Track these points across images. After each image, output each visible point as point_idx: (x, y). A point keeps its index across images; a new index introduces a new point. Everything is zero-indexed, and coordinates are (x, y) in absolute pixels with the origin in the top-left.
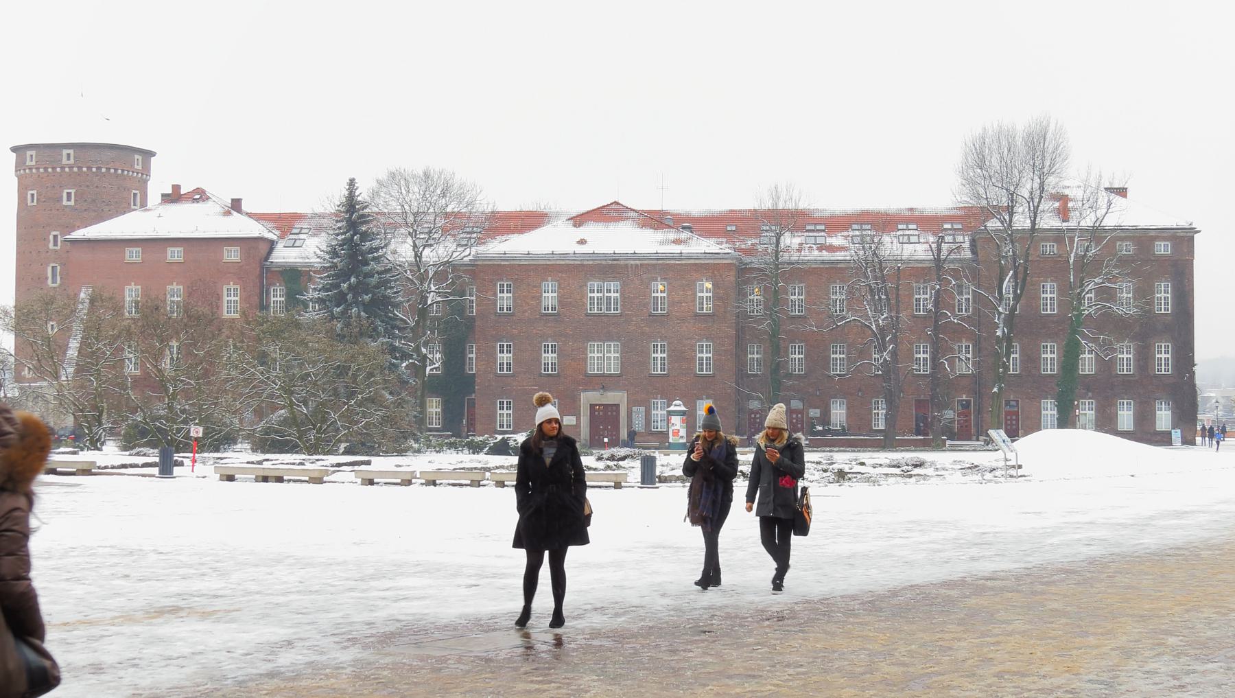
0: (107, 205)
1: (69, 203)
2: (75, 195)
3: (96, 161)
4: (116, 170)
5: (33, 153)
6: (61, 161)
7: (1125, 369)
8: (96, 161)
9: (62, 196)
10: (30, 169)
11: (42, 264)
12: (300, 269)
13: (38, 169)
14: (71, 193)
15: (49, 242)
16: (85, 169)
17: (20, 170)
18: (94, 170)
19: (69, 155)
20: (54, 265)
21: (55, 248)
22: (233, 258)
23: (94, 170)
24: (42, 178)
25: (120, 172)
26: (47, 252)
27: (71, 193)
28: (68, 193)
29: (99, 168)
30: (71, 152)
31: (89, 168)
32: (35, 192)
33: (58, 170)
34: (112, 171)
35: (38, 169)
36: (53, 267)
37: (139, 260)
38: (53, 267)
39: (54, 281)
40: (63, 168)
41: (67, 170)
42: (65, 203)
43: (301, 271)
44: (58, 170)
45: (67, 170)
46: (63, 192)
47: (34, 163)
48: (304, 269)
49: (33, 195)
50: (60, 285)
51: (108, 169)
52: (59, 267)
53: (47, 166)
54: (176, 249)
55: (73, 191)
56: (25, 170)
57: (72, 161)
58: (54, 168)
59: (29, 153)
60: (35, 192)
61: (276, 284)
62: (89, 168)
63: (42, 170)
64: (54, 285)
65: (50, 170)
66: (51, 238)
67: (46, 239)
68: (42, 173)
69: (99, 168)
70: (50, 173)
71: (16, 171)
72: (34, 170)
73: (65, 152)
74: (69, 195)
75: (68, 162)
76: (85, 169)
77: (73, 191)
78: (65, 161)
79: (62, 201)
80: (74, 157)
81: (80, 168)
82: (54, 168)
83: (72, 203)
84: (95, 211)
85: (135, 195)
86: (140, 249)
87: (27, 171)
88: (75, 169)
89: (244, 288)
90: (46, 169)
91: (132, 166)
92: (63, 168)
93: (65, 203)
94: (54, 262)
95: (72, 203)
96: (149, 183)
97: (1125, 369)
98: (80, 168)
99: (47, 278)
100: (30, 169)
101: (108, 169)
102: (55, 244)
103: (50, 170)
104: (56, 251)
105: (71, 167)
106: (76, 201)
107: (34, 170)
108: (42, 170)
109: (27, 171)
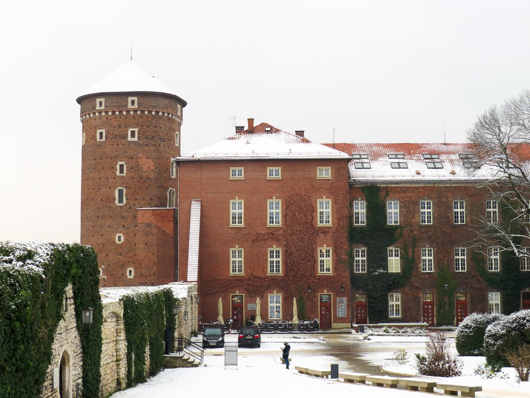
0: (163, 141)
1: (133, 139)
2: (138, 133)
3: (155, 107)
4: (168, 114)
5: (103, 100)
6: (126, 105)
7: (526, 267)
8: (155, 107)
9: (127, 134)
10: (100, 112)
11: (110, 188)
12: (378, 185)
13: (107, 112)
14: (134, 131)
15: (116, 170)
16: (146, 113)
17: (85, 115)
18: (154, 113)
19: (133, 102)
20: (121, 188)
21: (122, 175)
22: (324, 176)
23: (154, 113)
24: (110, 120)
25: (171, 115)
26: (115, 178)
27: (134, 131)
28: (132, 132)
29: (157, 112)
30: (135, 99)
31: (150, 112)
32: (103, 131)
33: (124, 113)
34: (166, 114)
35: (107, 112)
36: (119, 190)
37: (242, 177)
38: (119, 190)
39: (121, 201)
40: (128, 111)
41: (132, 113)
42: (130, 139)
43: (380, 187)
44: (124, 113)
45: (132, 113)
46: (128, 130)
47: (103, 107)
48: (382, 186)
49: (101, 134)
50: (126, 204)
51: (163, 113)
52: (125, 191)
53: (115, 110)
54: (274, 169)
55: (136, 130)
56: (94, 113)
57: (136, 106)
58: (121, 112)
59: (98, 100)
60: (103, 131)
61: (358, 199)
62: (150, 112)
63: (110, 113)
64: (121, 205)
65: (117, 113)
66: (118, 167)
67: (114, 168)
68: (111, 116)
69: (157, 112)
70: (117, 116)
71: (82, 116)
72: (103, 114)
73: (130, 99)
74: (133, 133)
75: (133, 107)
76: (146, 113)
77: (136, 130)
78: (130, 106)
79: (127, 137)
80: (138, 103)
81: (143, 112)
82: (121, 112)
83: (136, 139)
84: (154, 145)
85: (177, 135)
86: (243, 169)
87: (97, 114)
88: (139, 113)
89: (335, 201)
90: (113, 112)
91: (176, 113)
92: (128, 111)
93: (130, 139)
94: (121, 186)
95: (136, 139)
96: (181, 126)
97: (526, 267)
98: (143, 112)
99: (114, 199)
100: (100, 112)
101: (163, 113)
102: (122, 171)
103: (117, 113)
104: (122, 177)
105: (135, 111)
106: (139, 137)
107: (103, 114)
108: (110, 113)
109: (97, 114)
